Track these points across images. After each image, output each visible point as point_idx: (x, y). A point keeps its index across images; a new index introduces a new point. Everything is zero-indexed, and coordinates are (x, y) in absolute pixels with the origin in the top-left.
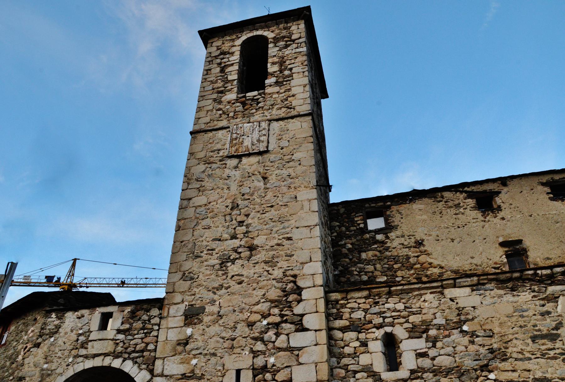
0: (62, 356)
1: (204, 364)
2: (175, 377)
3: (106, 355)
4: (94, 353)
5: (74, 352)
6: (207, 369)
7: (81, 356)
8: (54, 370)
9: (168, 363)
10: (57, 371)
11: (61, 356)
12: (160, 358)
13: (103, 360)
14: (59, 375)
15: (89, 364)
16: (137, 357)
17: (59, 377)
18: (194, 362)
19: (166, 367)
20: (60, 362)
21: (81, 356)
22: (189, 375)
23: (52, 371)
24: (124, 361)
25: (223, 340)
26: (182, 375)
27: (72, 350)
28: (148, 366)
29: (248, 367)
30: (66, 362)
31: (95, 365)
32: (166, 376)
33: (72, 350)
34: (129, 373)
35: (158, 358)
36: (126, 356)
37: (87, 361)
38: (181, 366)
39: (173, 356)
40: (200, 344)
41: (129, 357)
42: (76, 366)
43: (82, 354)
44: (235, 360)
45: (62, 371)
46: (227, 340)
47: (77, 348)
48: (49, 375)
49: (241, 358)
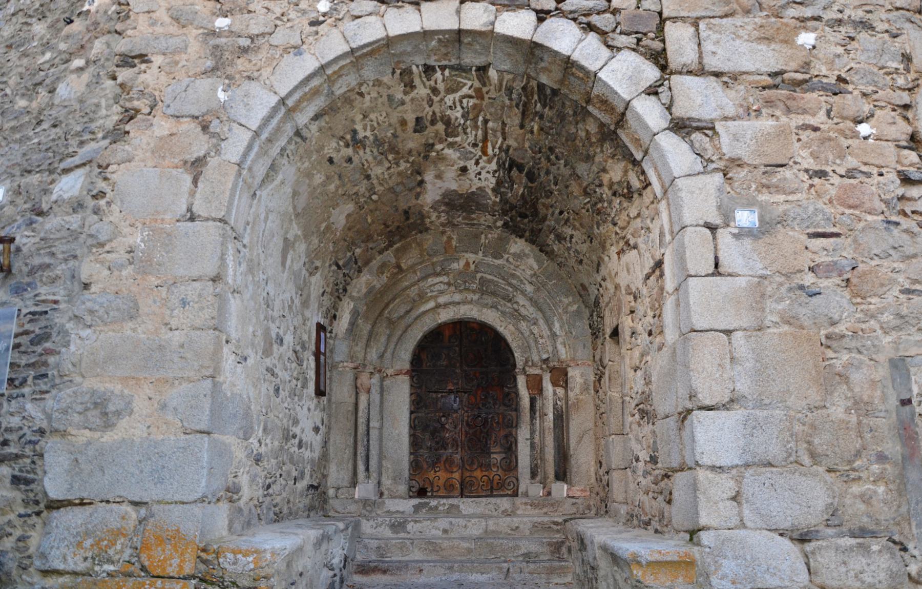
1: (840, 50)
2: (751, 78)
6: (853, 65)
8: (263, 35)
10: (278, 38)
12: (683, 19)
13: (458, 12)
14: (286, 50)
17: (289, 58)
18: (806, 39)
19: (708, 47)
22: (799, 76)
23: (252, 38)
24: (541, 20)
28: (639, 40)
30: (304, 12)
32: (717, 75)
34: (575, 57)
35: (674, 19)
38: (763, 47)
39: (726, 16)
41: (557, 9)
42: (349, 26)
45: (296, 40)
48: (245, 50)
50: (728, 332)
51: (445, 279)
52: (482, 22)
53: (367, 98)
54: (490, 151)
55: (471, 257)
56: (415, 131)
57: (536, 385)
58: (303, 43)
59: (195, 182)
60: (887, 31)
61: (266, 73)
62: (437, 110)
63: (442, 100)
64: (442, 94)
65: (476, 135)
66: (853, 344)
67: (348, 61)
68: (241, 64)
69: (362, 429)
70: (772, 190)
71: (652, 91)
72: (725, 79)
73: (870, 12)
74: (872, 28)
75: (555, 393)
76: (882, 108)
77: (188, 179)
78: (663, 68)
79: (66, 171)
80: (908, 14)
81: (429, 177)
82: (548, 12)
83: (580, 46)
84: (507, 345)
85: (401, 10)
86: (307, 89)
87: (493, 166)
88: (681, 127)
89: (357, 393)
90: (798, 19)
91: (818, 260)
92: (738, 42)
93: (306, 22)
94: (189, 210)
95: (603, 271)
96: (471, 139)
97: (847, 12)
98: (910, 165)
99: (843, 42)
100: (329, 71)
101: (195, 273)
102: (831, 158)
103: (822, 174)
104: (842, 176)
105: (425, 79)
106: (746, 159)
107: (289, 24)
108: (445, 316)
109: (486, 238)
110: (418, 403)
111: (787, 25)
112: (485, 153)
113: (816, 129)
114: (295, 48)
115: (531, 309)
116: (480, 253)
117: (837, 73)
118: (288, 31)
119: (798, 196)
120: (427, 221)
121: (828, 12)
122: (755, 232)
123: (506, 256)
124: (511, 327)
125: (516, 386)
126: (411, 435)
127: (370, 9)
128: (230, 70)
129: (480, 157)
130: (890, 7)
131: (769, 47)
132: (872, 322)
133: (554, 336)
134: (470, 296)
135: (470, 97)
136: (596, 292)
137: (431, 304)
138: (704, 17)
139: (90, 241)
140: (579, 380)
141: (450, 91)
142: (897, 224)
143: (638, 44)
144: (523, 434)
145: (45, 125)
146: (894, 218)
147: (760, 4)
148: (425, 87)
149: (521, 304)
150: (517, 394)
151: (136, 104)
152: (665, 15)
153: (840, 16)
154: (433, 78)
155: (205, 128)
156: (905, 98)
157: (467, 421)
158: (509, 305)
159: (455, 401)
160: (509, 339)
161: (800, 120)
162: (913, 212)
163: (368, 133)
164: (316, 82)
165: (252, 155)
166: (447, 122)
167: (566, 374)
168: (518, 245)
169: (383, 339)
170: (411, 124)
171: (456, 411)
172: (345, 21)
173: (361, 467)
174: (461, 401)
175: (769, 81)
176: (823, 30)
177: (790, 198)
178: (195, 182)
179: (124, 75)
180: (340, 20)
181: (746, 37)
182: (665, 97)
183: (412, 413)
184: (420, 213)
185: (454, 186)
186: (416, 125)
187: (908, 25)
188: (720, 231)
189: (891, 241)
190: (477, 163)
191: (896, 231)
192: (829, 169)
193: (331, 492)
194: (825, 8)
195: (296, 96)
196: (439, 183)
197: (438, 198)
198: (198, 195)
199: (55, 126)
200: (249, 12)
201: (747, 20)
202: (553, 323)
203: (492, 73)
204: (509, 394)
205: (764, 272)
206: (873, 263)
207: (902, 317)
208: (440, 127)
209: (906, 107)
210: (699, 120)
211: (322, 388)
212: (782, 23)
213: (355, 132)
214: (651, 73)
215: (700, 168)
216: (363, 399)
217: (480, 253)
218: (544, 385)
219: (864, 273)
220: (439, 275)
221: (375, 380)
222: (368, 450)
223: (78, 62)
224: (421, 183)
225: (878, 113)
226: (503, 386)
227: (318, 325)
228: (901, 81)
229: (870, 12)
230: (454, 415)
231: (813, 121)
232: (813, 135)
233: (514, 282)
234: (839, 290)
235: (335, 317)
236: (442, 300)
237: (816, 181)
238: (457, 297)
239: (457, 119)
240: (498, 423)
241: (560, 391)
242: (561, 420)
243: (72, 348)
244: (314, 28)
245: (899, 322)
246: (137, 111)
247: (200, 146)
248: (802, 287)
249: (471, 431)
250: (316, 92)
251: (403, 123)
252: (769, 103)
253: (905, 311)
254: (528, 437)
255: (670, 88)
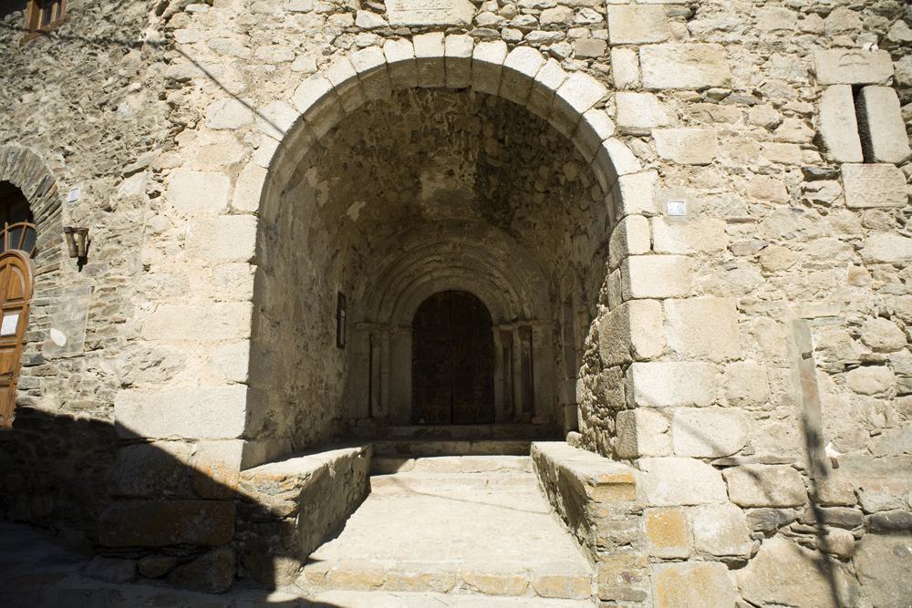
0: (301, 29)
1: (756, 68)
2: (681, 93)
3: (445, 29)
4: (409, 22)
5: (339, 19)
6: (766, 80)
7: (366, 30)
9: (652, 60)
10: (297, 65)
11: (296, 26)
14: (306, 75)
15: (399, 51)
16: (549, 42)
17: (307, 82)
19: (646, 68)
20: (297, 43)
21: (366, 30)
22: (722, 91)
23: (277, 65)
24: (510, 49)
25: (795, 14)
26: (700, 91)
27: (330, 13)
28: (590, 64)
29: (883, 78)
31: (421, 54)
32: (655, 91)
33: (330, 13)
36: (517, 35)
37: (390, 43)
40: (733, 20)
42: (355, 55)
43: (368, 26)
44: (842, 62)
46: (807, 13)
47: (346, 10)
48: (270, 75)
49: (858, 59)
50: (662, 299)
51: (438, 258)
52: (463, 52)
53: (372, 116)
54: (471, 158)
55: (456, 240)
56: (412, 142)
57: (508, 336)
58: (318, 68)
59: (233, 183)
60: (796, 52)
61: (288, 94)
62: (429, 125)
63: (432, 116)
64: (433, 112)
65: (460, 145)
66: (763, 309)
67: (355, 84)
68: (269, 86)
69: (375, 373)
70: (697, 185)
71: (602, 106)
72: (660, 95)
73: (782, 36)
74: (784, 50)
75: (523, 345)
76: (791, 116)
77: (228, 179)
78: (611, 86)
79: (128, 175)
80: (814, 37)
81: (424, 178)
82: (516, 42)
83: (542, 70)
84: (484, 305)
85: (397, 42)
86: (323, 107)
87: (474, 169)
88: (624, 134)
89: (371, 346)
90: (721, 43)
91: (735, 241)
92: (671, 63)
93: (320, 53)
94: (229, 205)
95: (560, 252)
96: (456, 148)
97: (763, 36)
98: (812, 163)
99: (759, 62)
100: (340, 93)
101: (235, 257)
102: (747, 158)
103: (738, 172)
104: (755, 173)
105: (418, 99)
106: (676, 160)
107: (306, 53)
108: (438, 288)
109: (469, 226)
110: (418, 354)
111: (712, 48)
112: (467, 159)
113: (734, 135)
114: (313, 73)
115: (504, 281)
116: (465, 238)
117: (753, 87)
118: (305, 59)
119: (720, 190)
120: (423, 213)
121: (746, 36)
122: (684, 219)
123: (484, 240)
124: (488, 294)
125: (492, 339)
126: (413, 377)
127: (372, 41)
128: (258, 91)
129: (464, 163)
130: (799, 31)
131: (697, 66)
132: (779, 291)
133: (521, 302)
134: (457, 271)
135: (454, 113)
136: (554, 267)
137: (427, 278)
138: (642, 44)
139: (149, 231)
140: (541, 335)
141: (438, 109)
142: (802, 211)
143: (589, 67)
144: (498, 376)
145: (110, 137)
146: (798, 207)
147: (690, 33)
148: (419, 107)
149: (497, 275)
150: (493, 345)
151: (183, 119)
152: (612, 41)
153: (756, 40)
154: (425, 99)
155: (240, 139)
156: (809, 107)
158: (487, 277)
160: (487, 304)
161: (719, 127)
162: (815, 201)
163: (374, 144)
164: (329, 102)
165: (280, 160)
166: (435, 132)
167: (531, 331)
168: (493, 232)
169: (391, 305)
170: (409, 136)
172: (352, 50)
173: (375, 402)
175: (697, 95)
176: (742, 52)
177: (712, 191)
178: (233, 183)
179: (173, 95)
180: (348, 50)
181: (678, 59)
182: (610, 111)
183: (413, 360)
184: (418, 207)
185: (443, 186)
186: (412, 137)
187: (813, 46)
188: (654, 218)
189: (796, 226)
190: (461, 168)
191: (800, 217)
192: (745, 167)
193: (352, 422)
194: (744, 34)
195: (314, 113)
196: (432, 184)
197: (431, 195)
198: (236, 193)
199: (118, 138)
200: (274, 43)
201: (678, 45)
202: (521, 292)
203: (472, 95)
205: (692, 251)
206: (781, 243)
207: (804, 287)
208: (432, 139)
209: (809, 115)
210: (637, 128)
211: (342, 342)
212: (708, 47)
213: (363, 142)
214: (599, 91)
215: (639, 168)
216: (376, 351)
217: (465, 238)
218: (514, 338)
219: (773, 252)
220: (433, 255)
221: (385, 336)
222: (380, 390)
223: (135, 85)
224: (419, 183)
225: (787, 120)
227: (339, 293)
228: (807, 93)
229: (782, 36)
231: (731, 127)
232: (733, 140)
233: (490, 260)
234: (751, 265)
235: (353, 288)
236: (435, 274)
237: (734, 177)
238: (447, 273)
239: (444, 131)
241: (527, 344)
242: (528, 364)
243: (136, 317)
244: (327, 57)
245: (801, 291)
246: (184, 125)
247: (237, 154)
248: (722, 263)
250: (330, 110)
251: (403, 135)
252: (695, 113)
253: (806, 282)
254: (502, 378)
255: (616, 104)
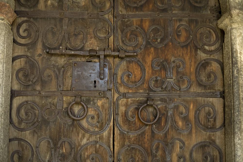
157: (125, 114)
159: (101, 75)
171: (103, 95)
174: (113, 75)
183: (13, 94)
204: (205, 64)
226: (196, 49)
230: (100, 103)
240: (186, 119)
249: (133, 135)
